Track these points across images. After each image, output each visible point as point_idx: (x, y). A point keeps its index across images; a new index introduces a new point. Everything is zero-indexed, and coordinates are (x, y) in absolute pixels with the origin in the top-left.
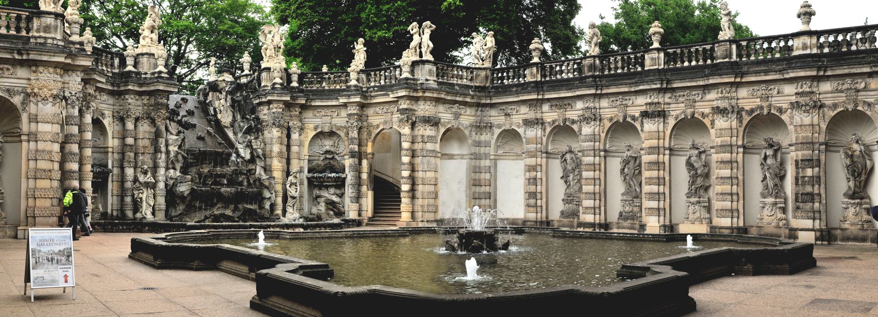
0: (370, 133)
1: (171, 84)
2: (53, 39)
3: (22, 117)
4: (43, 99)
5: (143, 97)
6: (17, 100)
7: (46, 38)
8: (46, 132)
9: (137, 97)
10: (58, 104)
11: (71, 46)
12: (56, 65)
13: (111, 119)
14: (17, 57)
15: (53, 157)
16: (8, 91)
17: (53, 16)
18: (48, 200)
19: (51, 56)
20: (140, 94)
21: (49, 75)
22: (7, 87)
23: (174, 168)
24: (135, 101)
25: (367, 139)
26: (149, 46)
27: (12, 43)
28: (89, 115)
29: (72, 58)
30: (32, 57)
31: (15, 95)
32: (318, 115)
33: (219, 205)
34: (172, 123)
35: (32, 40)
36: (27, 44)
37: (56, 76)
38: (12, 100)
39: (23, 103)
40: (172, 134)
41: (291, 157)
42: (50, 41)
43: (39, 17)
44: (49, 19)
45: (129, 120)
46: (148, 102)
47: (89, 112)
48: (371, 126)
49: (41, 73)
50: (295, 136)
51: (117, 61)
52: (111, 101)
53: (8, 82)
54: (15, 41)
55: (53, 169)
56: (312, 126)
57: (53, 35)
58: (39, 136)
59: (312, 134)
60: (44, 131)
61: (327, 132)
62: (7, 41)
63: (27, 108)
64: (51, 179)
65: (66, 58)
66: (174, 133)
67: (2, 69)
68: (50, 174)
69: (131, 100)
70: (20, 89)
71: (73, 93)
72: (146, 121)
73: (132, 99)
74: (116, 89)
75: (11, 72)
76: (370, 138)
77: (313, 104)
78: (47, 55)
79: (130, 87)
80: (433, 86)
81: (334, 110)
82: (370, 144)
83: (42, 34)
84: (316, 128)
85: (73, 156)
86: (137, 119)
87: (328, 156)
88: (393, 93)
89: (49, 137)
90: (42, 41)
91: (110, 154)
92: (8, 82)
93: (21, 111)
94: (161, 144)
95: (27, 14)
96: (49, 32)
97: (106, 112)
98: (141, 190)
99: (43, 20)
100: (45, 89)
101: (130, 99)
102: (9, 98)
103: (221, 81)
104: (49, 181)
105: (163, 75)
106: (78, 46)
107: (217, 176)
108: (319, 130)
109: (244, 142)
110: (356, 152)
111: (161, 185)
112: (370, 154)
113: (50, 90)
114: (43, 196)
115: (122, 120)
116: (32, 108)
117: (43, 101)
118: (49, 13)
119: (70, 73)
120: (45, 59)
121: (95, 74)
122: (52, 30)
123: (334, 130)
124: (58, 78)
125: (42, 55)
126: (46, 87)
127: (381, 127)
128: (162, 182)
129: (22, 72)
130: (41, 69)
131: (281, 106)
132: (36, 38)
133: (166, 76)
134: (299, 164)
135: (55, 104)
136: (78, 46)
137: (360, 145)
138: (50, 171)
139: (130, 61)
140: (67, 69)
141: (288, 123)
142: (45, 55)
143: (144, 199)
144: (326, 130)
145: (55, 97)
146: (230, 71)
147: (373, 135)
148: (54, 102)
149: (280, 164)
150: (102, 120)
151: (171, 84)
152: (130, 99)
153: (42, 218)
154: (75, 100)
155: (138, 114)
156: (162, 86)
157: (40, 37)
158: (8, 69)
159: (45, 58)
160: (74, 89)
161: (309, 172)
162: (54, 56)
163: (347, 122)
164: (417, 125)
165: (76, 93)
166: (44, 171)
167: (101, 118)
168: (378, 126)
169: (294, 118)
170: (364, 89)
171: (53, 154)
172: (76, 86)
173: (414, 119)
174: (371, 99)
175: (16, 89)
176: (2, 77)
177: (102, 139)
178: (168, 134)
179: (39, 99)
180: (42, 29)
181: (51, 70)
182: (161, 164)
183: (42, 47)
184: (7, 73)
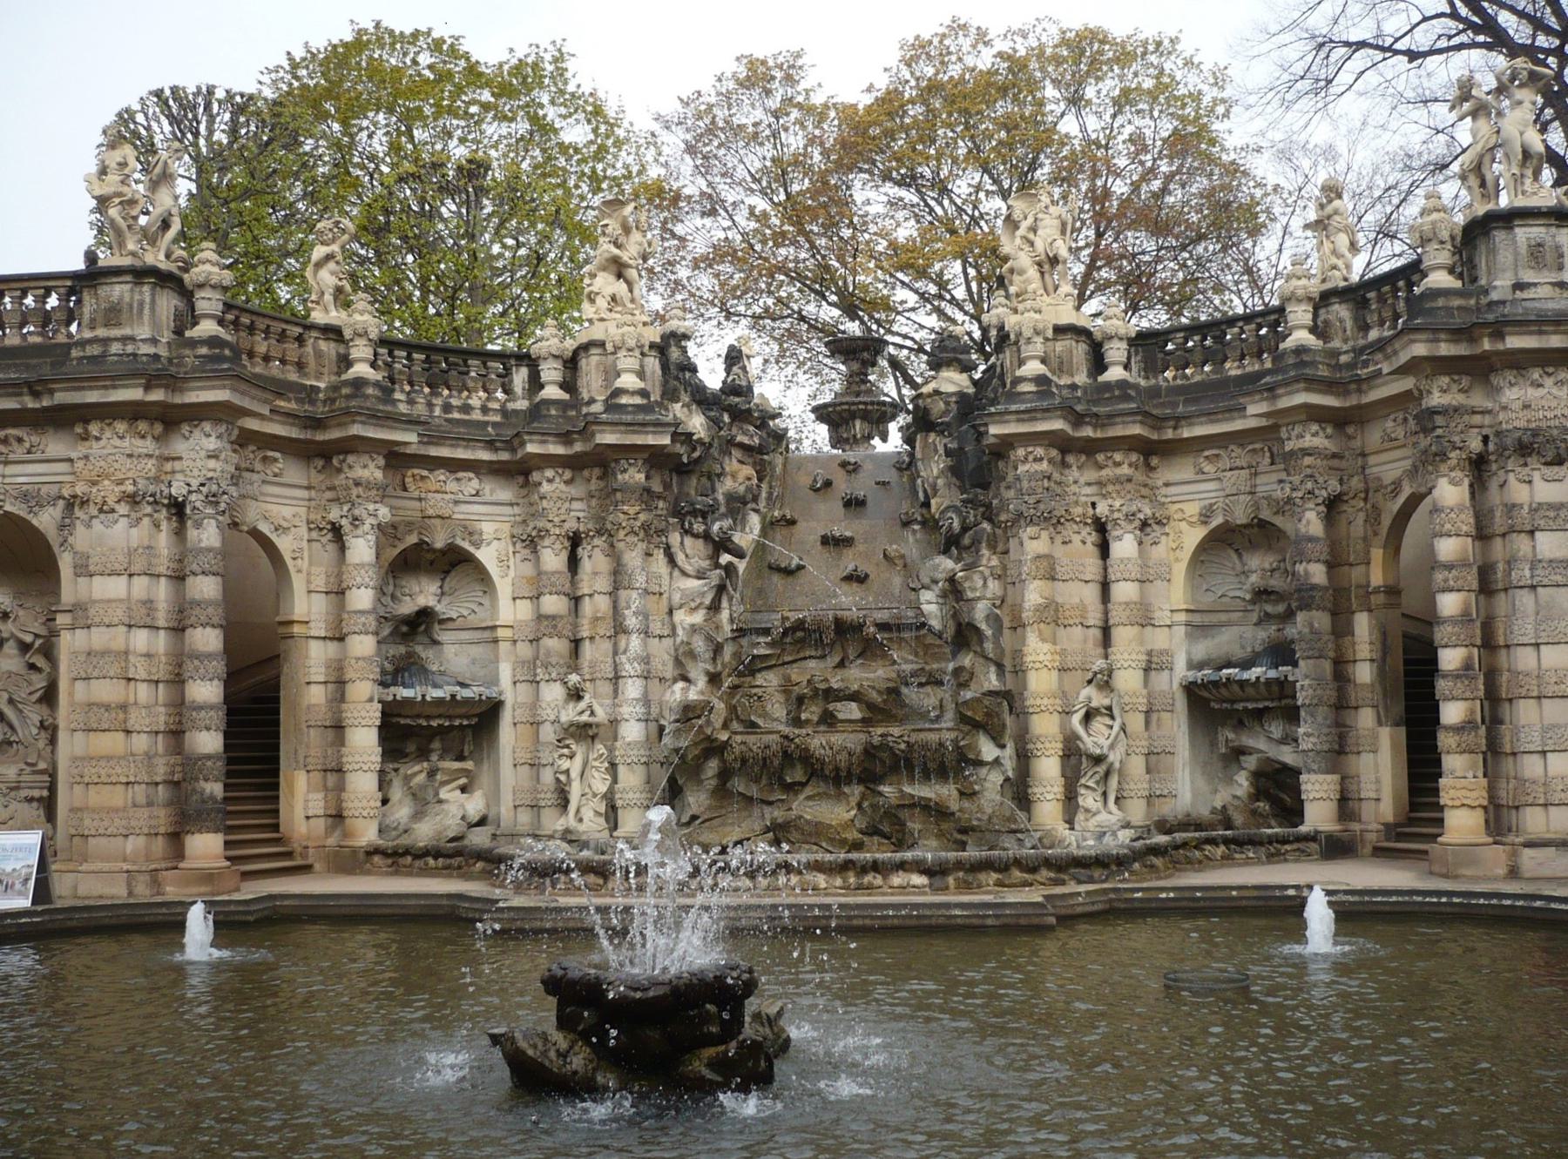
0: (1374, 516)
1: (644, 425)
2: (125, 340)
3: (61, 564)
4: (101, 511)
5: (586, 473)
6: (46, 520)
7: (106, 341)
8: (109, 601)
9: (568, 474)
10: (146, 521)
11: (187, 352)
12: (133, 413)
13: (505, 546)
14: (31, 404)
15: (132, 670)
16: (25, 497)
17: (128, 278)
18: (120, 788)
19: (105, 387)
20: (574, 464)
21: (117, 442)
22: (25, 487)
23: (686, 679)
24: (562, 487)
25: (1365, 539)
26: (602, 320)
27: (28, 367)
28: (361, 540)
29: (166, 387)
30: (62, 397)
31: (42, 506)
32: (1208, 468)
33: (808, 791)
34: (688, 541)
35: (75, 353)
36: (63, 364)
37: (139, 442)
38: (35, 522)
39: (62, 527)
40: (684, 574)
41: (1111, 622)
42: (115, 348)
43: (95, 286)
44: (117, 288)
45: (547, 542)
46: (602, 484)
47: (359, 532)
48: (1377, 491)
49: (98, 439)
50: (1124, 546)
51: (520, 377)
52: (505, 493)
53: (23, 474)
54: (34, 361)
55: (136, 703)
56: (1193, 509)
57: (127, 331)
58: (92, 612)
59: (1193, 536)
60: (107, 596)
61: (1245, 526)
62: (16, 365)
63: (71, 540)
64: (128, 732)
65: (148, 388)
66: (688, 569)
67: (5, 441)
68: (121, 716)
69: (552, 485)
70: (54, 490)
71: (195, 483)
72: (597, 541)
73: (550, 481)
74: (505, 456)
75: (27, 445)
76: (1376, 534)
77: (1186, 433)
78: (97, 388)
79: (531, 448)
80: (1551, 305)
81: (1257, 446)
82: (1377, 554)
83: (101, 332)
84: (1205, 517)
85: (196, 662)
86: (575, 541)
87: (1269, 608)
88: (1387, 357)
89: (119, 612)
90: (94, 350)
91: (504, 647)
92: (23, 474)
93: (56, 549)
94: (629, 607)
95: (69, 283)
96: (119, 325)
97: (488, 528)
98: (568, 747)
99: (103, 291)
100: (106, 482)
101: (545, 484)
102: (29, 517)
103: (929, 395)
104: (121, 735)
105: (624, 400)
106: (204, 351)
107: (830, 695)
108: (1217, 521)
109: (935, 582)
110: (1314, 587)
111: (632, 731)
112: (1377, 591)
113: (120, 482)
114: (104, 779)
115: (532, 544)
116: (81, 537)
117: (102, 516)
118: (117, 272)
119: (185, 428)
120: (93, 400)
121: (354, 422)
122: (125, 316)
123: (1266, 514)
124: (148, 445)
125: (83, 388)
126: (107, 477)
127: (1407, 491)
128: (633, 722)
129: (56, 445)
130: (94, 428)
131: (1040, 451)
132: (83, 343)
133: (638, 400)
134: (1142, 643)
135: (139, 520)
136: (204, 351)
137: (1332, 565)
138: (124, 707)
139: (551, 372)
140: (171, 420)
141: (1094, 505)
142: (91, 388)
143: (574, 774)
144: (1241, 517)
145: (133, 500)
146: (959, 361)
147: (1386, 521)
148: (133, 515)
149: (1046, 647)
150: (471, 549)
151: (644, 425)
152: (545, 484)
153: (103, 840)
154: (198, 504)
155: (571, 525)
156: (612, 432)
157: (90, 341)
158: (20, 440)
159: (92, 397)
160: (196, 472)
161: (1191, 665)
162: (114, 387)
163: (1281, 481)
164: (1494, 467)
165: (203, 485)
166: (107, 707)
167: (466, 545)
168: (1397, 487)
169: (1110, 488)
170: (1343, 359)
171: (132, 658)
172: (199, 463)
173: (1475, 445)
174: (1360, 391)
175: (44, 489)
176: (6, 463)
177: (486, 601)
178: (676, 573)
179: (93, 510)
180: (100, 319)
181: (121, 427)
182: (627, 666)
183: (101, 370)
184: (19, 452)
